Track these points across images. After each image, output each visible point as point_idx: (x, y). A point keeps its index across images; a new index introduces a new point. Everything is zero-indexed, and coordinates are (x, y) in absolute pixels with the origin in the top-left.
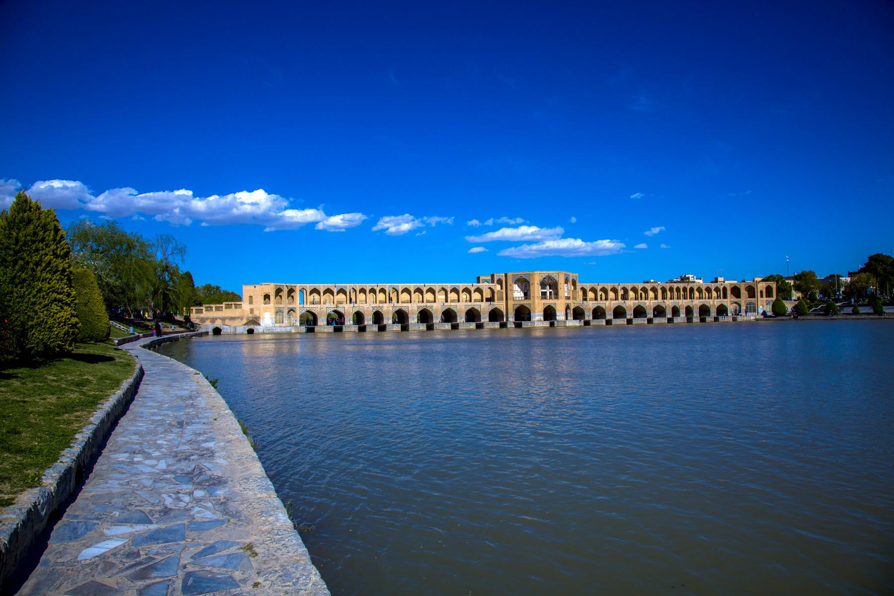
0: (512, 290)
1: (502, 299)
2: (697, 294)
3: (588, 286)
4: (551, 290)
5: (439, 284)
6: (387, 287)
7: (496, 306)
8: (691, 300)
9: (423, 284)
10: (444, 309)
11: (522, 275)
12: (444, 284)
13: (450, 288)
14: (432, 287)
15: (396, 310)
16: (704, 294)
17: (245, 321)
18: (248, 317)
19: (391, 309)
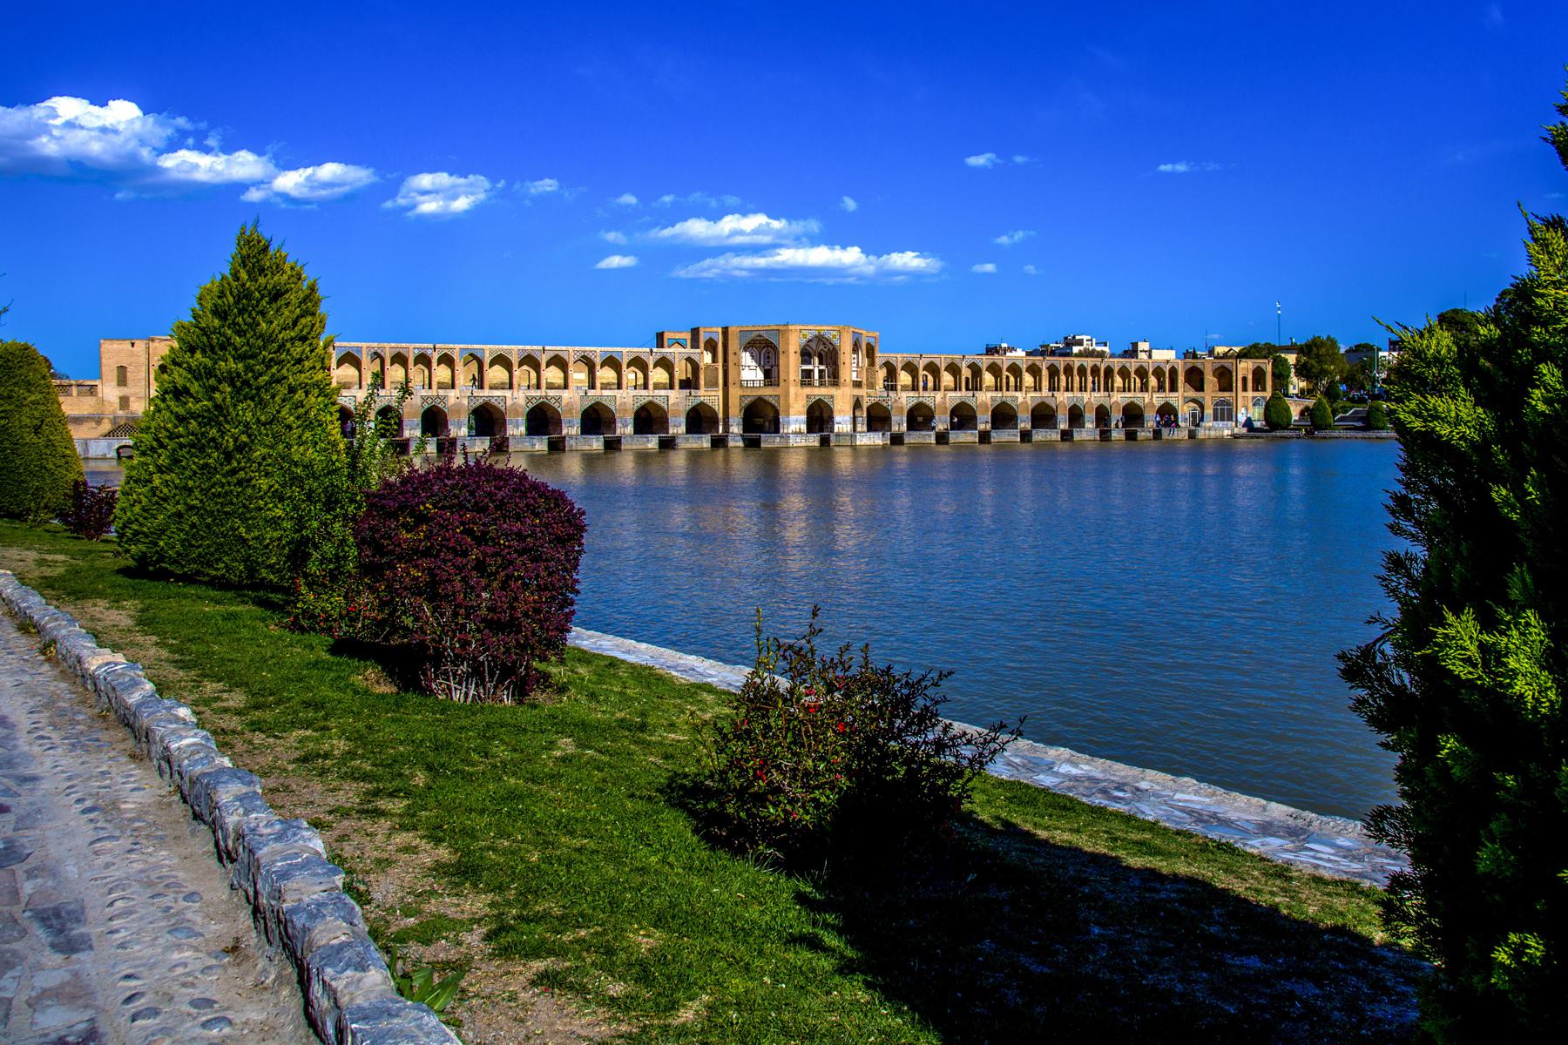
0: (738, 365)
1: (716, 385)
2: (1118, 381)
3: (900, 359)
4: (822, 367)
5: (577, 348)
6: (457, 351)
7: (702, 399)
8: (1107, 393)
9: (540, 348)
10: (587, 404)
11: (761, 333)
12: (588, 348)
13: (601, 356)
14: (560, 354)
15: (478, 404)
16: (1132, 380)
17: (106, 427)
18: (115, 418)
19: (465, 402)
